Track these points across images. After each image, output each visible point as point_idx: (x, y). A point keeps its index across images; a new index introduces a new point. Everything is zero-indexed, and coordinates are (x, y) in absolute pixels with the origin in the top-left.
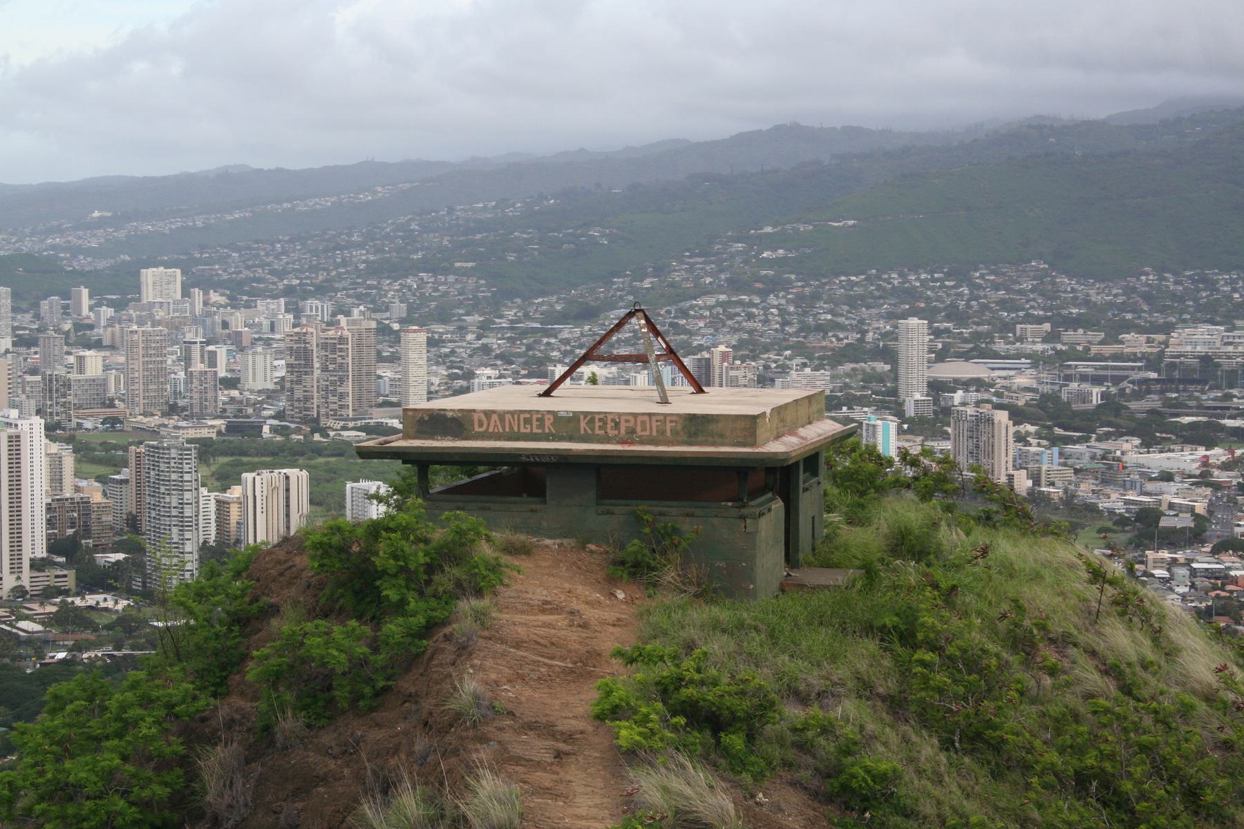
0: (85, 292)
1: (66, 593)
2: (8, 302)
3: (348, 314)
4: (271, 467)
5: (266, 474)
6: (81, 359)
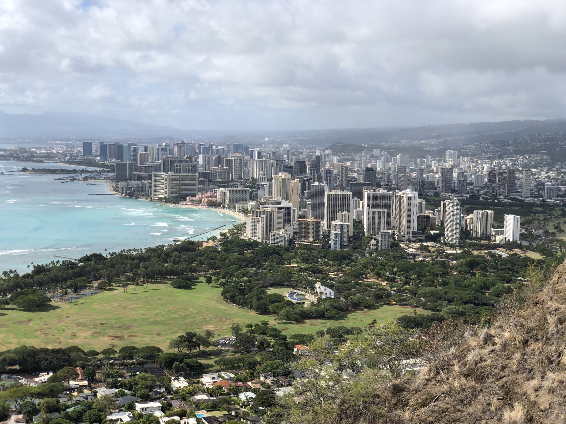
0: (430, 157)
5: (481, 212)
6: (428, 176)
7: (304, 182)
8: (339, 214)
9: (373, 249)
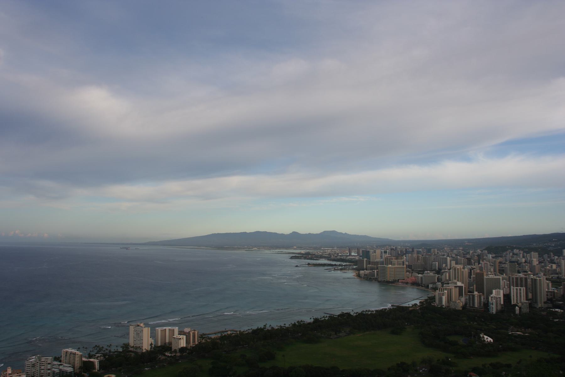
2: (537, 255)
6: (552, 266)
7: (471, 270)
8: (494, 291)
9: (517, 312)
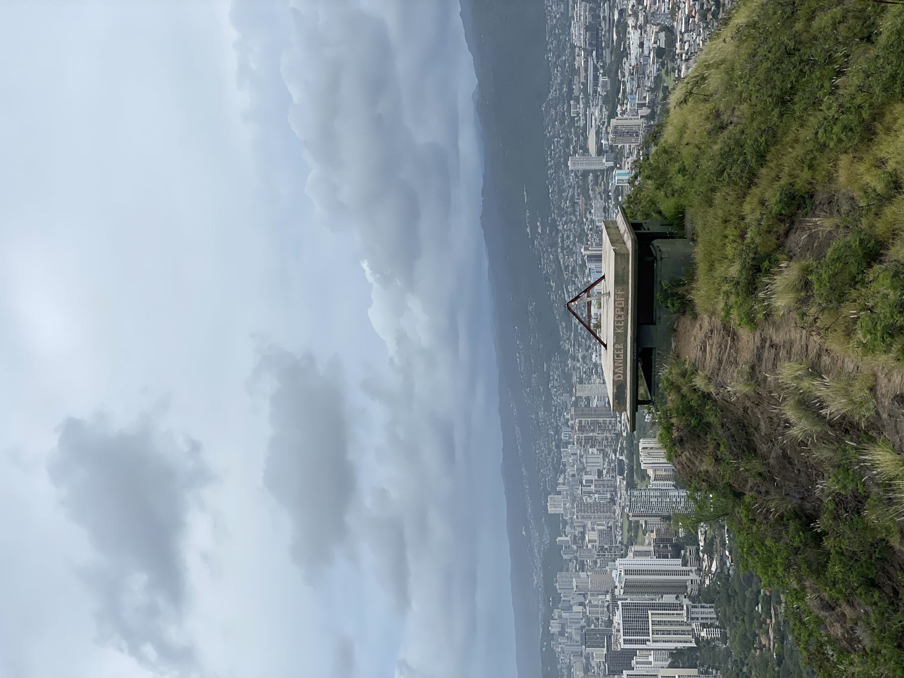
0: (559, 538)
1: (698, 550)
3: (568, 420)
4: (638, 456)
5: (641, 458)
6: (590, 541)
9: (717, 633)
